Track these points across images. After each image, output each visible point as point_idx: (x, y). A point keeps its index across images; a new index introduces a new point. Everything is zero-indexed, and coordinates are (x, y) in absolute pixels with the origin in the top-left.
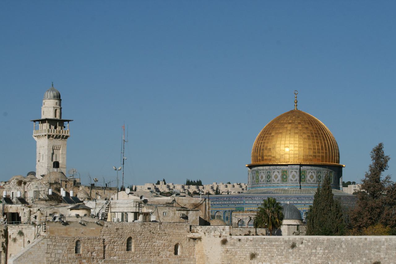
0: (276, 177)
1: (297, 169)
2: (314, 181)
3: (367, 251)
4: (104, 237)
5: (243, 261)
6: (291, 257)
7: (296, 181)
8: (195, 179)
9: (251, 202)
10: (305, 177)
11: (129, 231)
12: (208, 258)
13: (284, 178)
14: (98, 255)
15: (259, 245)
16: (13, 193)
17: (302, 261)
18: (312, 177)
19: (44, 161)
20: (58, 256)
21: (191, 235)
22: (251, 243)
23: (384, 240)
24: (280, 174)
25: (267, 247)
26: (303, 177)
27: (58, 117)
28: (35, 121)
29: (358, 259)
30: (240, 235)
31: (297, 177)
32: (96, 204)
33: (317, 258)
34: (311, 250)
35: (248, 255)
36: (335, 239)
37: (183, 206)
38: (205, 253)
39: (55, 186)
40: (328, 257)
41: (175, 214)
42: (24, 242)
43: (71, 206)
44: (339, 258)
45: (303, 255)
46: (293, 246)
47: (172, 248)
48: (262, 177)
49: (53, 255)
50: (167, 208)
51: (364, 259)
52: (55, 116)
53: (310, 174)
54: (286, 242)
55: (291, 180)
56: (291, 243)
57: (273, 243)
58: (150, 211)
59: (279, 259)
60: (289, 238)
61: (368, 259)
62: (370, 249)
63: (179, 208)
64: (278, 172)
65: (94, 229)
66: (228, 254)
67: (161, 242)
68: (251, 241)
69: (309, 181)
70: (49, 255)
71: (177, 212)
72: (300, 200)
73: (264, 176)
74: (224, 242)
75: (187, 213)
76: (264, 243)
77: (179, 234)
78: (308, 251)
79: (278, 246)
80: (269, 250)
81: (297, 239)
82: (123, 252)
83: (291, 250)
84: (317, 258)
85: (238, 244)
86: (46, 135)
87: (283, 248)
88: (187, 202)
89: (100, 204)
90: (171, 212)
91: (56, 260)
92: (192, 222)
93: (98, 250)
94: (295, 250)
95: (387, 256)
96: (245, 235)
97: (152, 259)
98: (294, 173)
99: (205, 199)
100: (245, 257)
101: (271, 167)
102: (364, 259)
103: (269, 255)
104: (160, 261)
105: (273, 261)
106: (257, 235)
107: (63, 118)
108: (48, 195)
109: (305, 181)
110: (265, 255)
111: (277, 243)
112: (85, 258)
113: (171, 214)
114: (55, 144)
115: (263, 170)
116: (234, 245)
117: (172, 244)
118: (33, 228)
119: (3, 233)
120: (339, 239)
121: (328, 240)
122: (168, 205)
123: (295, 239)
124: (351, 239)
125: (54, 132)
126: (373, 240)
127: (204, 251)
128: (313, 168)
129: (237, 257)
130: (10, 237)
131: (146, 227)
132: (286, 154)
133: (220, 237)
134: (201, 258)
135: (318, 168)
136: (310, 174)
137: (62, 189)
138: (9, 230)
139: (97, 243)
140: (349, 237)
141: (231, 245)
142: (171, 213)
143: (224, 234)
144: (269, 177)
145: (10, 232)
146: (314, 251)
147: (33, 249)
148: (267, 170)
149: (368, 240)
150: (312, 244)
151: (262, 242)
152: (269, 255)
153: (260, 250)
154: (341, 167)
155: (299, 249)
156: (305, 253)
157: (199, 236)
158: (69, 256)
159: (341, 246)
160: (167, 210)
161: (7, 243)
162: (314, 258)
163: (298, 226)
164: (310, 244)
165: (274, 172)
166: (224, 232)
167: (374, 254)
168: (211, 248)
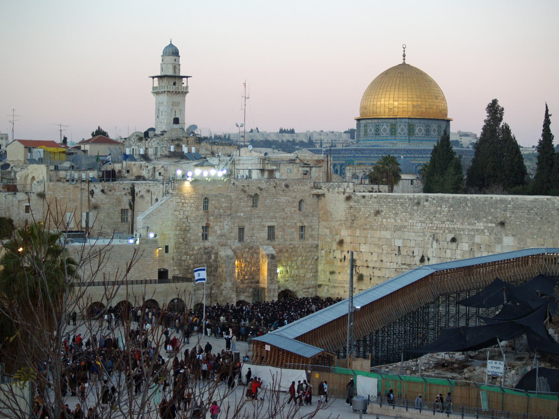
0: (385, 130)
1: (405, 123)
2: (422, 134)
3: (493, 210)
4: (231, 194)
5: (367, 217)
6: (416, 214)
7: (405, 134)
8: (288, 127)
9: (360, 155)
10: (413, 130)
12: (331, 214)
13: (393, 131)
14: (225, 212)
16: (133, 149)
17: (427, 218)
18: (420, 130)
19: (163, 117)
20: (186, 213)
21: (315, 191)
22: (375, 200)
23: (510, 199)
24: (389, 127)
25: (391, 204)
26: (411, 130)
27: (177, 74)
28: (153, 77)
29: (485, 217)
30: (364, 192)
31: (406, 131)
32: (220, 160)
33: (442, 216)
34: (437, 207)
35: (372, 211)
36: (461, 197)
37: (305, 162)
39: (176, 142)
40: (453, 215)
41: (298, 170)
42: (151, 199)
43: (195, 163)
44: (465, 217)
45: (427, 212)
46: (418, 203)
47: (297, 204)
48: (371, 130)
49: (182, 212)
50: (291, 165)
51: (490, 218)
52: (175, 72)
53: (419, 127)
54: (410, 199)
55: (400, 134)
56: (416, 201)
57: (398, 200)
58: (275, 168)
59: (404, 216)
60: (414, 196)
61: (494, 218)
62: (496, 208)
63: (302, 165)
64: (387, 125)
65: (221, 186)
66: (352, 211)
68: (375, 198)
69: (418, 134)
70: (177, 213)
71: (301, 169)
72: (409, 154)
73: (373, 130)
74: (348, 198)
75: (310, 170)
78: (432, 209)
79: (402, 204)
80: (394, 207)
81: (422, 197)
82: (249, 209)
83: (415, 208)
84: (442, 216)
85: (362, 201)
86: (165, 92)
87: (407, 205)
88: (310, 158)
89: (223, 160)
91: (185, 217)
92: (315, 179)
93: (225, 207)
94: (421, 207)
95: (513, 215)
96: (370, 192)
97: (277, 215)
98: (402, 126)
99: (327, 156)
100: (368, 213)
101: (380, 121)
102: (490, 218)
103: (394, 212)
104: (285, 217)
105: (397, 218)
106: (380, 192)
107: (182, 74)
108: (170, 152)
109: (413, 134)
110: (390, 211)
111: (401, 200)
112: (213, 216)
113: (295, 170)
115: (372, 123)
116: (357, 201)
118: (162, 186)
119: (130, 191)
120: (465, 198)
121: (453, 198)
122: (292, 161)
123: (420, 196)
124: (477, 198)
125: (172, 88)
126: (499, 199)
127: (328, 208)
128: (422, 121)
129: (361, 213)
130: (137, 194)
132: (394, 107)
133: (344, 193)
134: (324, 214)
135: (426, 121)
136: (419, 127)
137: (184, 146)
138: (135, 188)
139: (223, 200)
140: (475, 196)
141: (355, 202)
143: (348, 190)
144: (377, 130)
145: (137, 190)
146: (439, 209)
147: (161, 207)
148: (375, 123)
149: (494, 199)
150: (437, 202)
151: (387, 199)
152: (394, 212)
153: (385, 206)
154: (448, 121)
155: (424, 206)
156: (430, 210)
157: (323, 192)
158: (198, 213)
159: (466, 205)
160: (290, 166)
161: (133, 200)
162: (439, 216)
163: (412, 180)
164: (434, 202)
165: (383, 125)
167: (500, 213)
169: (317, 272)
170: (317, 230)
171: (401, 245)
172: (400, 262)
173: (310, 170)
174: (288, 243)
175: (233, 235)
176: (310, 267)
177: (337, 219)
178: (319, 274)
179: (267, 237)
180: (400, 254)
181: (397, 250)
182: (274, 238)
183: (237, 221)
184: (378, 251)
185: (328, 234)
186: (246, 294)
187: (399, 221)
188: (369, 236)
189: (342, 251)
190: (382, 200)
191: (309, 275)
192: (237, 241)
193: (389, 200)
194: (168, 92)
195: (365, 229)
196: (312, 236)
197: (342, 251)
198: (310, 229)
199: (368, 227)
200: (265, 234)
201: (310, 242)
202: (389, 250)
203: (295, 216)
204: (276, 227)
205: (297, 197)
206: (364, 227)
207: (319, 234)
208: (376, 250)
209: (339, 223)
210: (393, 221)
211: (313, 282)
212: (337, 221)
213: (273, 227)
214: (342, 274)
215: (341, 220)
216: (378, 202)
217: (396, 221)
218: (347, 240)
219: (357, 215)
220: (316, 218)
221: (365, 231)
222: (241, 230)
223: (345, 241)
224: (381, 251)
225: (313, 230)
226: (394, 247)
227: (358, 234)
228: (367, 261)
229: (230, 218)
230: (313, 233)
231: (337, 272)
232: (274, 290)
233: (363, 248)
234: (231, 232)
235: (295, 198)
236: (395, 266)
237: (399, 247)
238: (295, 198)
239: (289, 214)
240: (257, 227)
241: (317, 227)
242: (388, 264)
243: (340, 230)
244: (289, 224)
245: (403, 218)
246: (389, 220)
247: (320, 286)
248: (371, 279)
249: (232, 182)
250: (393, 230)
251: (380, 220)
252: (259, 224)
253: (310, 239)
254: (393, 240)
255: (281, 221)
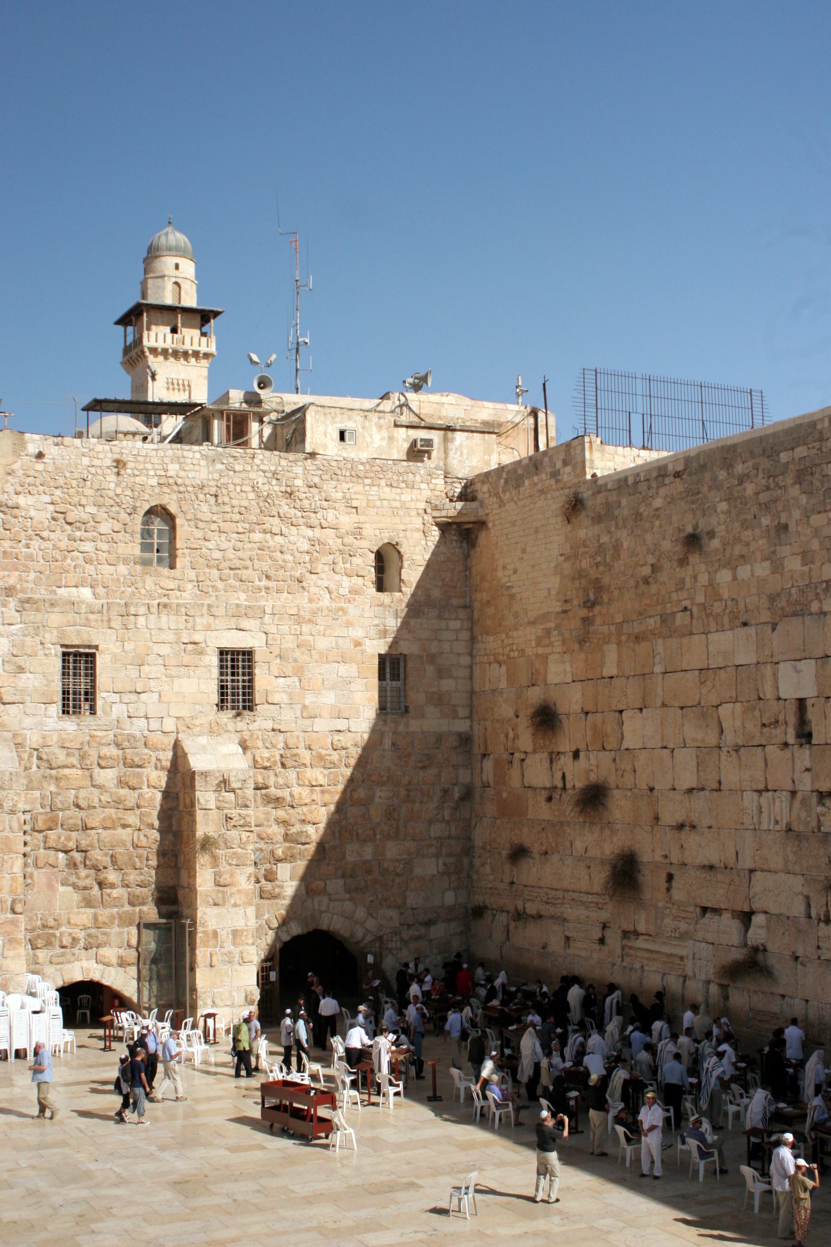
4: (22, 500)
11: (154, 481)
12: (512, 597)
15: (715, 486)
22: (679, 486)
35: (666, 545)
38: (504, 580)
57: (784, 457)
59: (817, 532)
67: (310, 533)
68: (677, 475)
76: (739, 468)
77: (397, 504)
80: (764, 497)
82: (123, 569)
90: (374, 429)
100: (651, 560)
103: (765, 521)
104: (306, 615)
105: (785, 551)
110: (745, 526)
114: (174, 376)
117: (365, 544)
129: (618, 566)
131: (238, 468)
141: (598, 519)
142: (377, 437)
152: (765, 521)
153: (723, 506)
166: (568, 469)
168: (524, 551)
169: (468, 850)
170: (466, 673)
171: (809, 691)
172: (806, 784)
173: (446, 440)
174: (322, 725)
175: (28, 681)
176: (437, 830)
177: (532, 615)
178: (477, 862)
179: (215, 698)
180: (805, 736)
181: (792, 720)
182: (249, 705)
183: (55, 619)
184: (700, 735)
185: (503, 684)
186: (110, 953)
187: (794, 564)
188: (658, 669)
189: (553, 757)
190: (707, 475)
191: (428, 867)
192: (55, 709)
193: (739, 468)
194: (154, 351)
195: (638, 638)
196: (438, 699)
197: (553, 757)
198: (430, 669)
199: (652, 623)
200: (206, 681)
201: (431, 722)
202: (753, 727)
203: (352, 610)
204: (257, 657)
205: (368, 530)
206: (637, 628)
207: (472, 693)
208: (693, 732)
209: (539, 630)
210: (763, 569)
211: (449, 898)
212: (532, 623)
213: (248, 654)
214: (555, 858)
215: (545, 617)
216: (691, 494)
217: (777, 567)
218: (571, 702)
219: (606, 580)
220: (455, 624)
221: (644, 645)
222: (79, 662)
223: (562, 708)
224: (712, 739)
225: (442, 673)
226: (774, 706)
227: (610, 669)
228: (651, 789)
229: (12, 603)
230: (447, 685)
231: (536, 849)
232: (235, 933)
233: (637, 730)
234: (21, 670)
235: (358, 532)
236: (779, 808)
237: (801, 703)
238: (358, 532)
239: (326, 602)
240: (165, 650)
241: (465, 660)
242: (750, 799)
243: (545, 658)
244: (322, 644)
245: (815, 545)
246: (744, 572)
247: (479, 912)
248: (670, 877)
249: (32, 449)
250: (765, 616)
251: (703, 579)
252: (170, 637)
253: (432, 711)
254: (768, 670)
255: (285, 628)
